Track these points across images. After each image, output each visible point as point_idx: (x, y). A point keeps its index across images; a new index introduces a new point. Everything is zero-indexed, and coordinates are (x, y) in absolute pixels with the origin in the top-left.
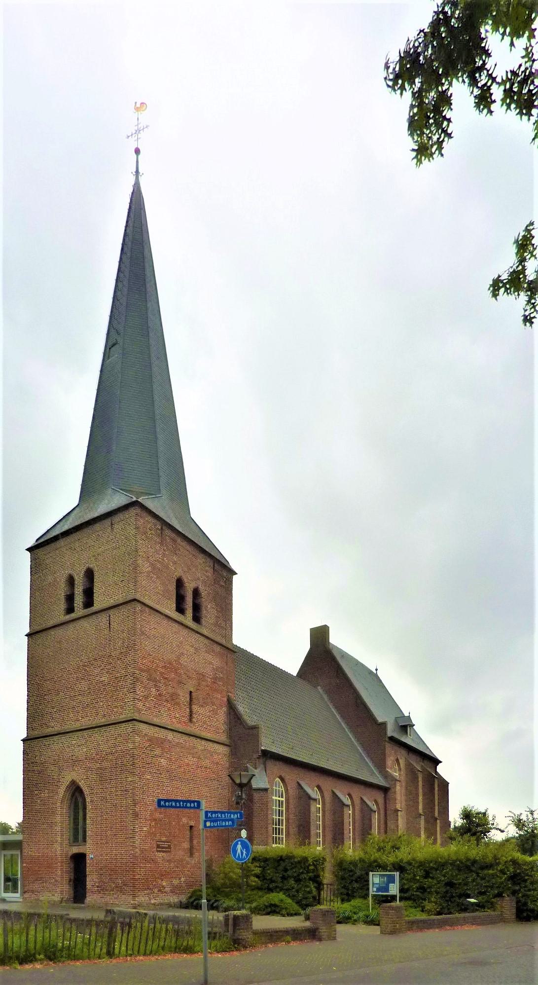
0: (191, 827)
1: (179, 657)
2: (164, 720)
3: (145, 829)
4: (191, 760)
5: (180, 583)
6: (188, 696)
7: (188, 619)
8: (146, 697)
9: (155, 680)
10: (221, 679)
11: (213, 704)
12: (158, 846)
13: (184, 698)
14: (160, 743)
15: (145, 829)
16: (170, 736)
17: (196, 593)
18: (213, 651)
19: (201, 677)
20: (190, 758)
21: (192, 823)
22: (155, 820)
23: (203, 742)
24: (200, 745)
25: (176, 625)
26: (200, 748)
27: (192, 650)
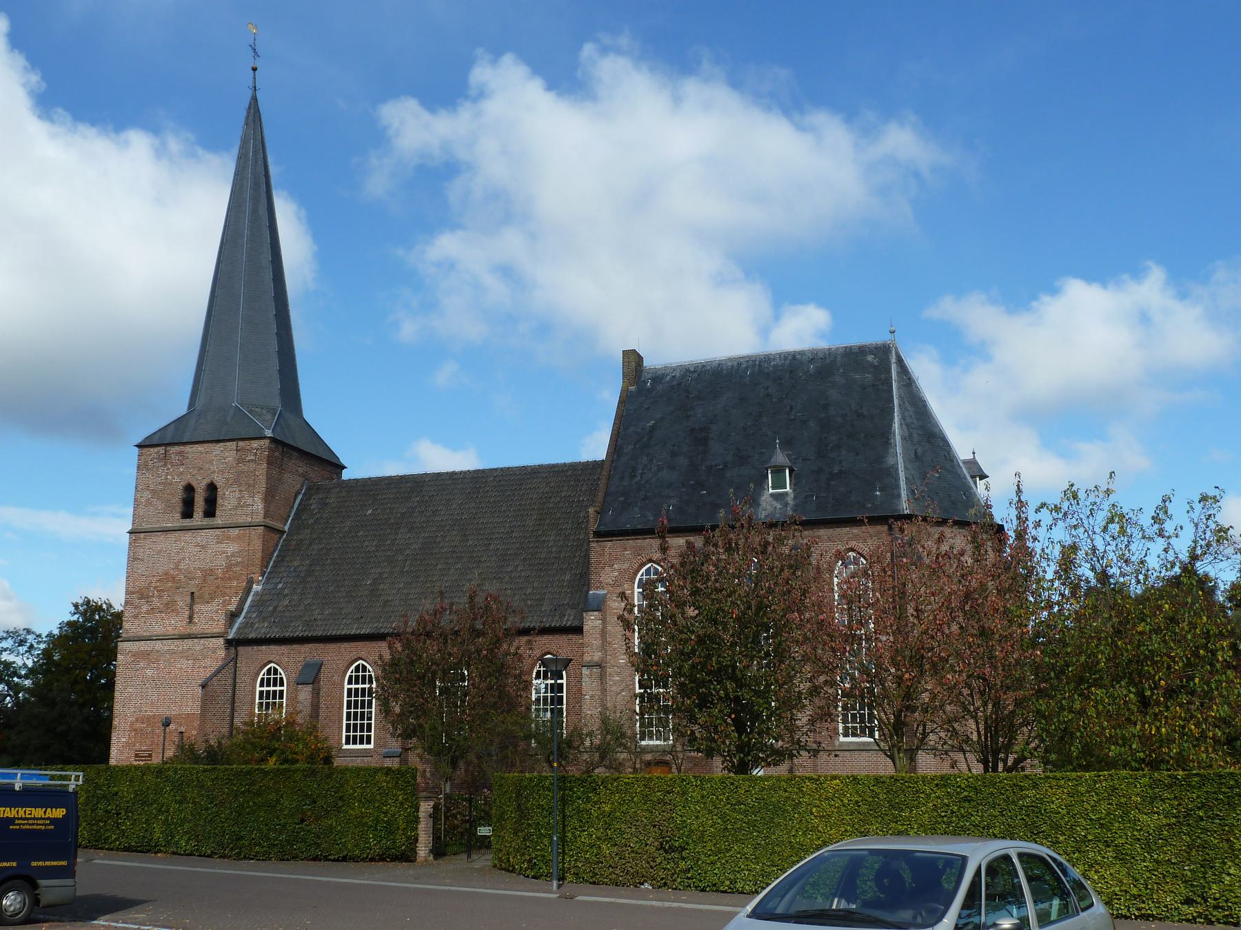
0: (182, 733)
1: (177, 565)
2: (158, 629)
3: (124, 740)
4: (184, 664)
5: (189, 489)
6: (188, 599)
7: (198, 518)
8: (136, 617)
9: (148, 597)
10: (237, 564)
11: (224, 594)
12: (137, 756)
13: (182, 602)
14: (146, 655)
15: (124, 740)
16: (158, 645)
17: (212, 488)
18: (228, 538)
19: (208, 573)
20: (184, 661)
21: (183, 729)
22: (135, 730)
23: (202, 641)
24: (197, 645)
25: (177, 534)
26: (198, 648)
27: (198, 549)
